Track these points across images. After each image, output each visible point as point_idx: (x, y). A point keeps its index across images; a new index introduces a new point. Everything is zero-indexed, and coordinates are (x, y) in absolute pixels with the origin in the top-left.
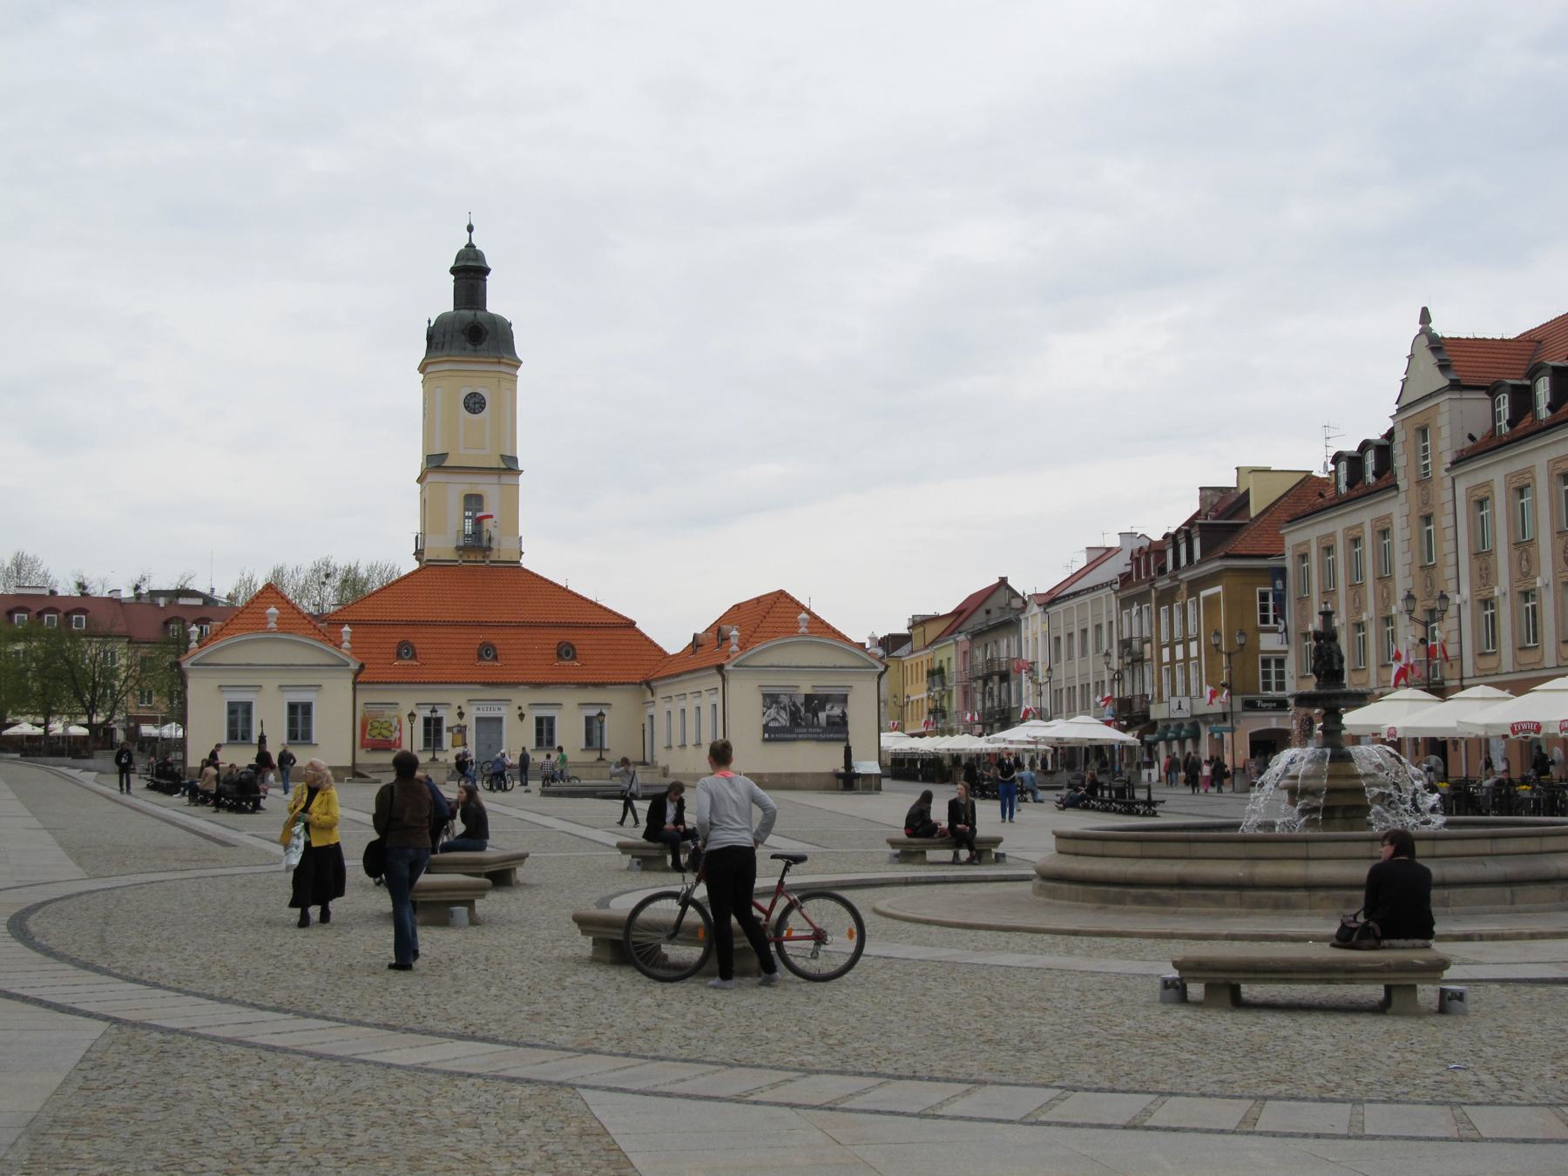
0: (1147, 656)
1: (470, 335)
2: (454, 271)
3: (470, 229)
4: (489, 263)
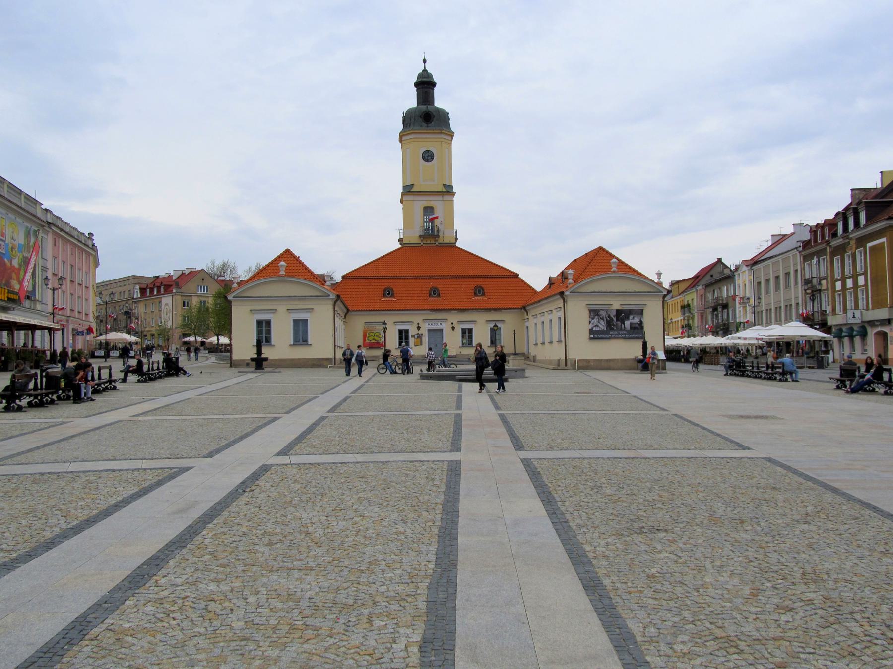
0: (824, 287)
1: (426, 118)
2: (416, 85)
3: (425, 61)
4: (435, 80)
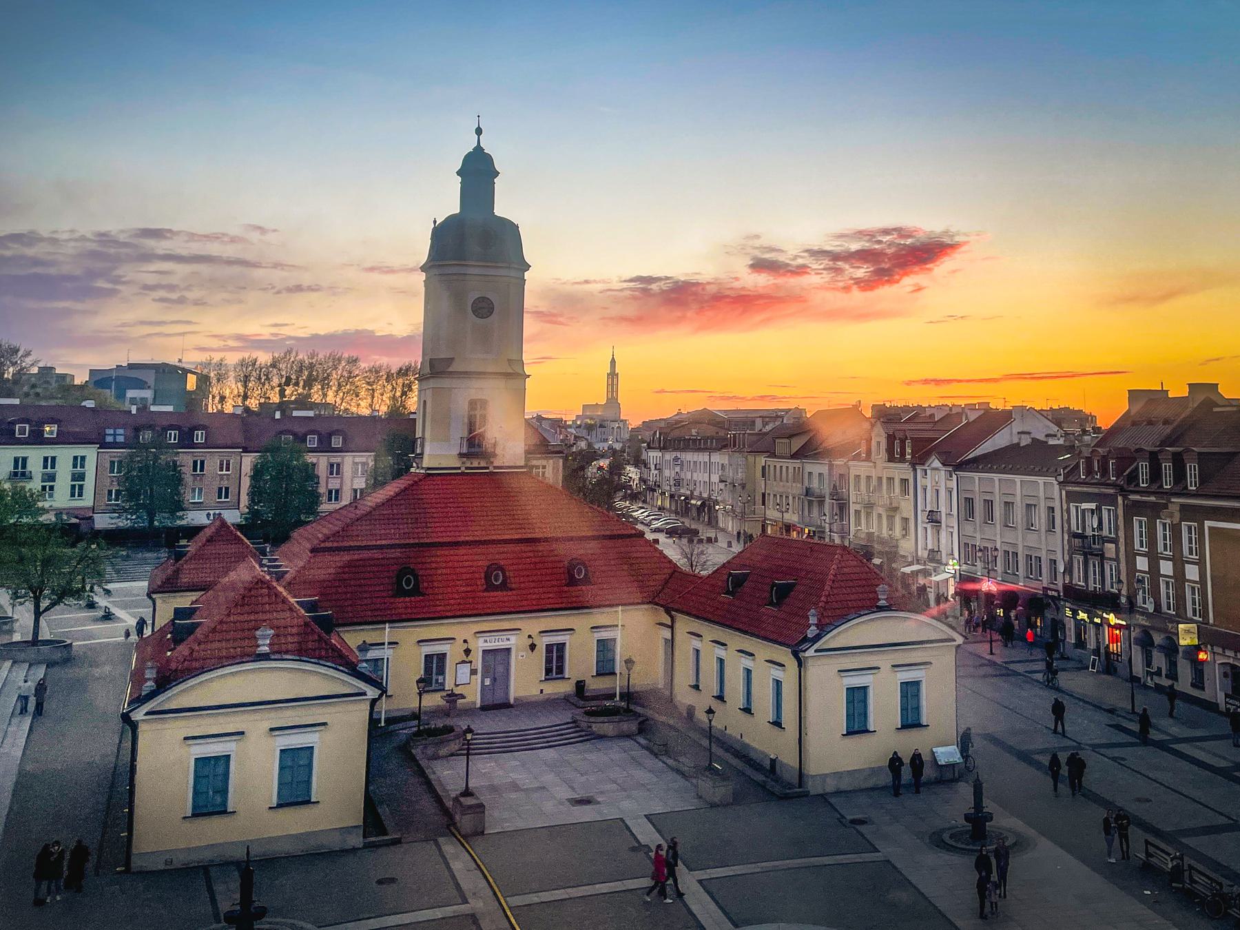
3: (479, 131)
